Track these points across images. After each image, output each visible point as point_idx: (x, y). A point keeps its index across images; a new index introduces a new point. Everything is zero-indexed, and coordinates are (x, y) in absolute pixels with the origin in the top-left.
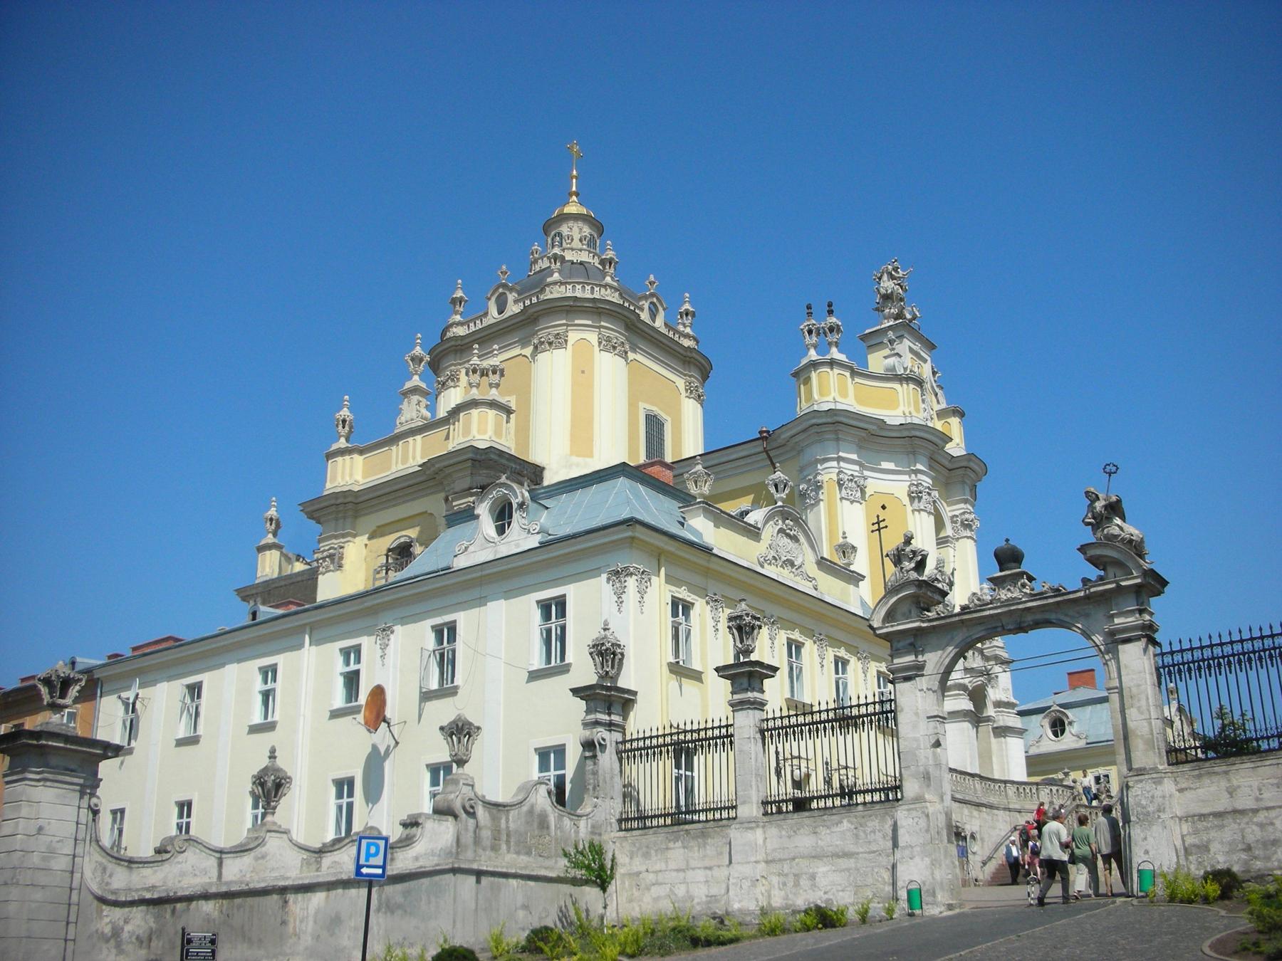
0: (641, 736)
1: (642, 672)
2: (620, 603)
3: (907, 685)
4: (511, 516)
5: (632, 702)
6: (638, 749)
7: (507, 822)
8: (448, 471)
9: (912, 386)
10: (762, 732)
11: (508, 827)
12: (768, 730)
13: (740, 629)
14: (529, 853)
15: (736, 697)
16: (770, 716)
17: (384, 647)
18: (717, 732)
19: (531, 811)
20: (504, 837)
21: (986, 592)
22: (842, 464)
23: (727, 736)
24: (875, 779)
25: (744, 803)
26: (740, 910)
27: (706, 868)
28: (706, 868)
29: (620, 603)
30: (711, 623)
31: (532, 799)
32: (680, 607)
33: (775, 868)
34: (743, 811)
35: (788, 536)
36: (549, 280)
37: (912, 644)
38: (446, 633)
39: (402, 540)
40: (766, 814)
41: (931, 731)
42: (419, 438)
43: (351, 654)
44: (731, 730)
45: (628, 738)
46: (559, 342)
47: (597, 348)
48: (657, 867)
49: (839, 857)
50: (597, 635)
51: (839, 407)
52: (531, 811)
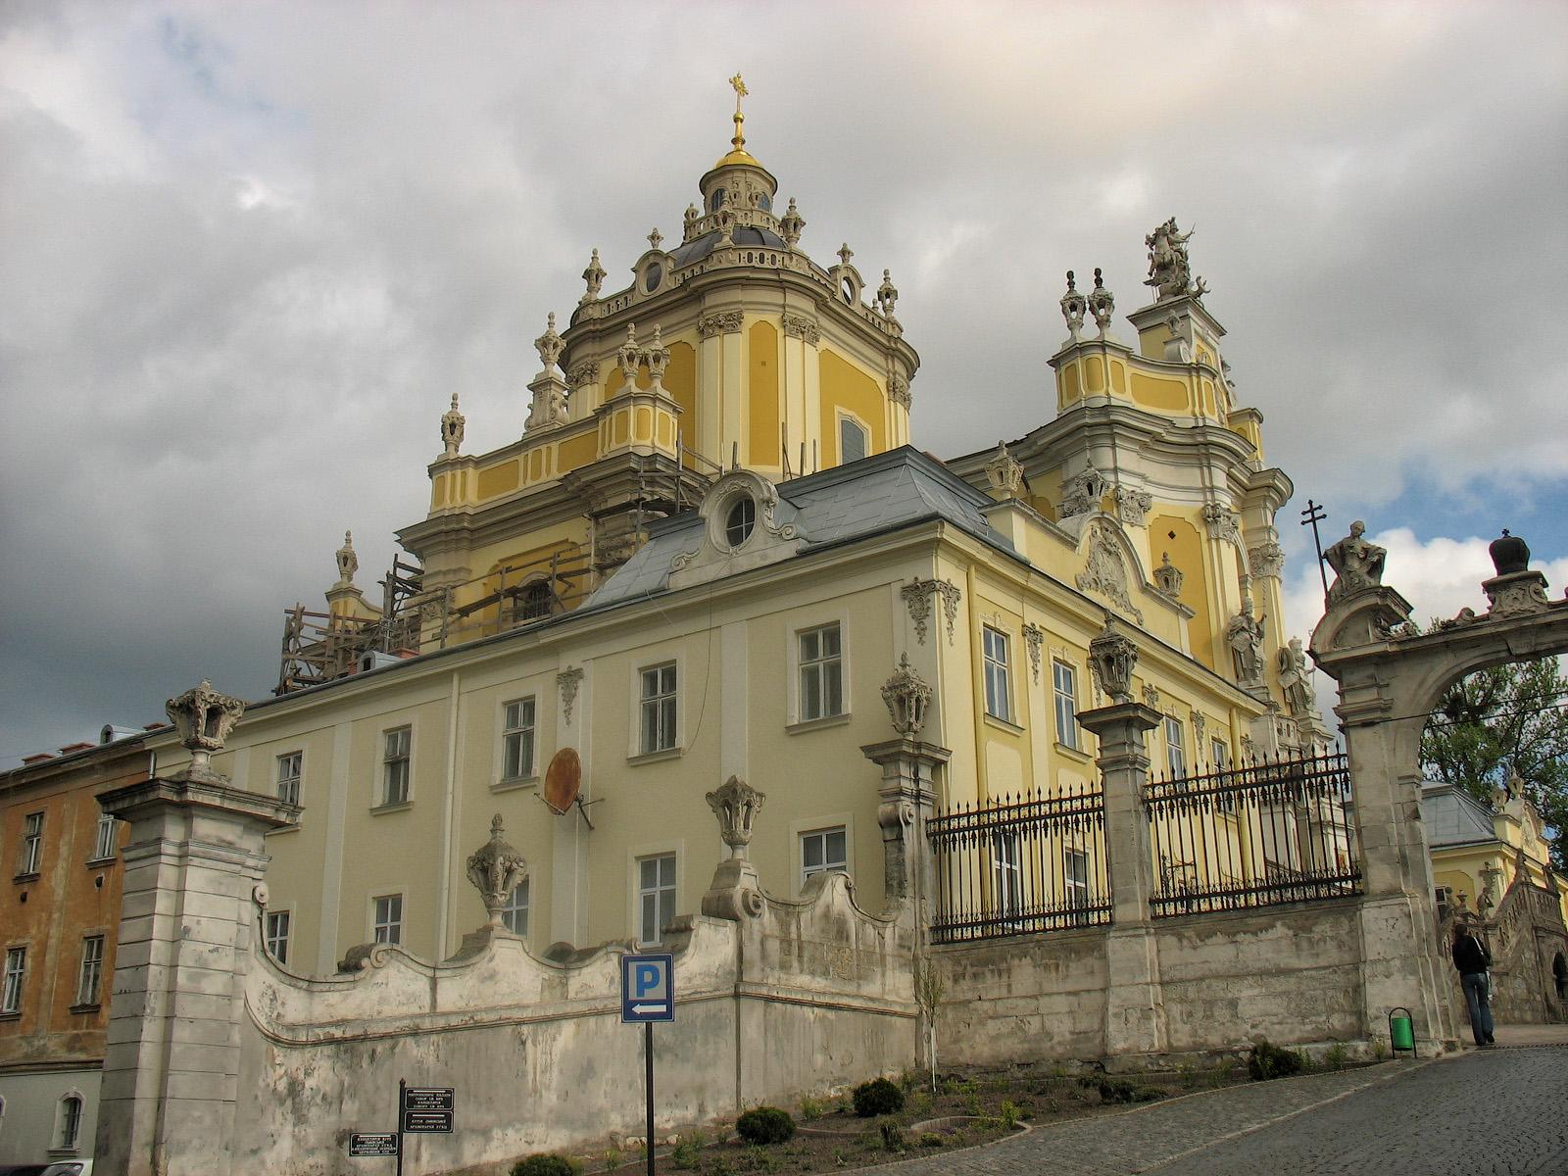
0: (964, 810)
1: (955, 723)
3: (1367, 733)
4: (751, 517)
5: (945, 763)
6: (959, 830)
7: (798, 929)
8: (598, 486)
9: (1205, 379)
10: (1145, 801)
11: (799, 936)
12: (1154, 800)
13: (1109, 660)
14: (825, 974)
15: (1106, 754)
16: (1158, 779)
17: (569, 698)
18: (1077, 804)
20: (795, 950)
21: (1481, 605)
22: (1121, 477)
24: (1214, 879)
25: (1126, 901)
26: (1127, 1051)
27: (1069, 993)
28: (1069, 993)
30: (1030, 663)
32: (996, 638)
33: (1174, 992)
34: (1122, 913)
35: (1110, 553)
36: (716, 246)
37: (1372, 677)
38: (661, 679)
39: (534, 577)
40: (1155, 918)
41: (1405, 798)
42: (555, 445)
43: (522, 710)
45: (945, 814)
46: (732, 323)
47: (781, 332)
48: (995, 994)
51: (1114, 402)
52: (826, 915)
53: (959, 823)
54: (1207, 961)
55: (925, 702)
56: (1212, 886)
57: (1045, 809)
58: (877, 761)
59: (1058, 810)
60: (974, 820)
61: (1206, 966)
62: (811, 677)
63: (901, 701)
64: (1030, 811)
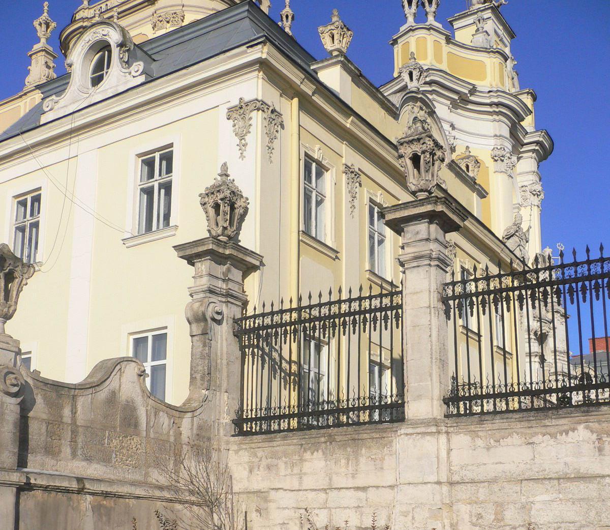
2: (243, 146)
7: (74, 412)
10: (445, 300)
18: (376, 303)
19: (112, 398)
23: (392, 308)
25: (419, 397)
27: (358, 489)
28: (358, 489)
29: (243, 146)
31: (112, 383)
32: (312, 168)
44: (397, 300)
45: (250, 312)
49: (568, 479)
50: (212, 182)
53: (263, 321)
54: (501, 463)
55: (239, 211)
56: (509, 385)
57: (344, 307)
58: (190, 260)
59: (358, 309)
60: (277, 318)
61: (500, 468)
62: (149, 192)
63: (217, 207)
64: (330, 310)
